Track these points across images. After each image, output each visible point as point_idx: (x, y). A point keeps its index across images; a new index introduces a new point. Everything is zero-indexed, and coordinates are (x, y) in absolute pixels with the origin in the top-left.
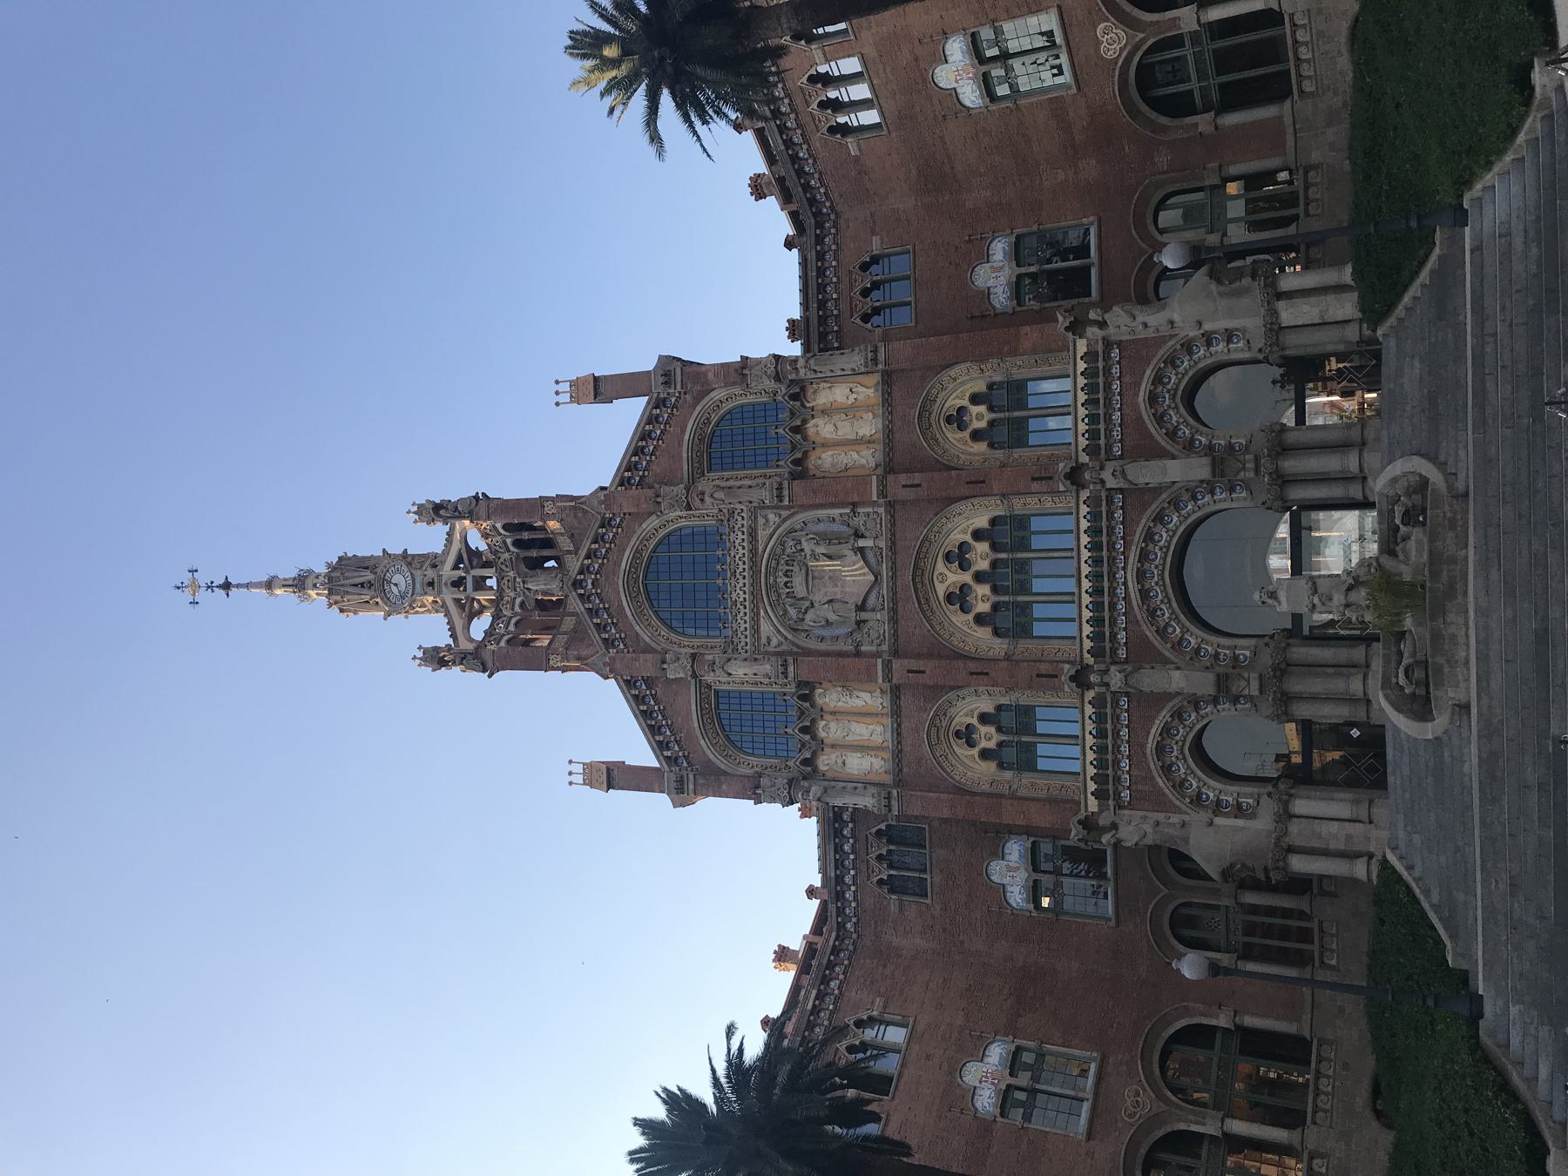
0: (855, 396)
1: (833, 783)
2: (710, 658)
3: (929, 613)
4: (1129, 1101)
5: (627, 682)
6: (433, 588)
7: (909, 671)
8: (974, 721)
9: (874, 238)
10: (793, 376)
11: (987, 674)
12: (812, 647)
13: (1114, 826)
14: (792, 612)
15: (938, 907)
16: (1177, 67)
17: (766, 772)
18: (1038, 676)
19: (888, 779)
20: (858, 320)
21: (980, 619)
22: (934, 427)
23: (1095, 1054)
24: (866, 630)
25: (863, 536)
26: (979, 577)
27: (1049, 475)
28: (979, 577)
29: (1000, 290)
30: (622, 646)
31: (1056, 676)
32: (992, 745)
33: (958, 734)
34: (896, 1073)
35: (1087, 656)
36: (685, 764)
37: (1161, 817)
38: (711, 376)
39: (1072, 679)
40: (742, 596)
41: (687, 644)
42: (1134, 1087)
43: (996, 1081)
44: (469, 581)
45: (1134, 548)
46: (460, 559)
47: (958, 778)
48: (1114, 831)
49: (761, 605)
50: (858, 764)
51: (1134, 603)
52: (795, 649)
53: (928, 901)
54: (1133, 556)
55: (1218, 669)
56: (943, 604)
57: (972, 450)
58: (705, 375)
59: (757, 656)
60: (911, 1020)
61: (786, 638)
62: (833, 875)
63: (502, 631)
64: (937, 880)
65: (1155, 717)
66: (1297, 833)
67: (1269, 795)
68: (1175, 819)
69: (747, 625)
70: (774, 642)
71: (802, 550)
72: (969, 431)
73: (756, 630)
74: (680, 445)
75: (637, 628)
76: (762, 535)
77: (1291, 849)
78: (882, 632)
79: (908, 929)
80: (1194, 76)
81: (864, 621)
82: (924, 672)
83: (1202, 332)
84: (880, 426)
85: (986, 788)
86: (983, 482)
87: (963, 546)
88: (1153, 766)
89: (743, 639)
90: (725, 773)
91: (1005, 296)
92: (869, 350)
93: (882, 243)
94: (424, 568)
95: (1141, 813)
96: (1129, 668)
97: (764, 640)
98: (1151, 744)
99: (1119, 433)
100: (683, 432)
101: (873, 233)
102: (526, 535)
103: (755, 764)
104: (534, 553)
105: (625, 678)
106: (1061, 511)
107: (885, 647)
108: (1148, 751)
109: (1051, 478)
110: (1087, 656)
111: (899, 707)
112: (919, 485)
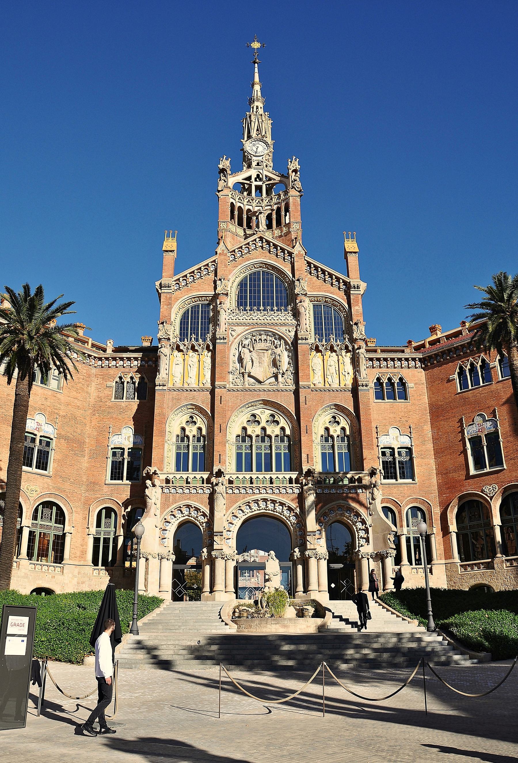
0: (346, 375)
1: (168, 359)
2: (226, 302)
3: (247, 406)
4: (33, 488)
5: (214, 261)
6: (256, 165)
7: (221, 397)
8: (198, 425)
9: (413, 384)
10: (356, 347)
11: (220, 432)
12: (231, 351)
13: (154, 486)
14: (246, 342)
15: (110, 404)
16: (476, 516)
17: (172, 327)
18: (220, 455)
19: (170, 385)
20: (377, 376)
21: (244, 429)
22: (331, 411)
23: (51, 473)
24: (239, 377)
25: (282, 377)
26: (264, 429)
27: (309, 462)
28: (264, 429)
29: (388, 440)
30: (231, 259)
31: (220, 462)
32: (187, 433)
33: (192, 417)
34: (50, 388)
35: (229, 476)
36: (176, 288)
37: (159, 505)
38: (357, 308)
39: (220, 470)
40: (255, 318)
41: (232, 290)
42: (39, 490)
43: (38, 429)
44: (260, 183)
45: (277, 497)
46: (270, 179)
47: (172, 417)
48: (152, 486)
49: (250, 327)
50: (177, 371)
51: (253, 497)
52: (230, 343)
53: (113, 400)
54: (274, 497)
55: (224, 531)
56: (251, 412)
57: (320, 427)
58: (357, 305)
59: (227, 324)
60: (61, 391)
61: (235, 339)
62: (124, 356)
63: (237, 200)
64: (123, 405)
65: (202, 504)
66: (154, 563)
67: (169, 551)
68: (158, 513)
69: (241, 320)
70: (233, 333)
71: (276, 348)
72: (329, 426)
73: (238, 325)
74: (325, 291)
75: (240, 267)
76: (283, 329)
77: (147, 559)
78: (238, 384)
79: (100, 390)
80: (471, 523)
81: (243, 376)
82: (221, 403)
83: (369, 527)
84: (332, 386)
85: (168, 429)
86: (307, 433)
87: (278, 423)
88: (181, 503)
89: (234, 318)
90: (171, 308)
91: (386, 442)
92: (366, 382)
93: (411, 388)
94: (266, 161)
95: (160, 498)
96: (224, 495)
97: (235, 328)
98: (189, 502)
99: (327, 492)
100: (331, 293)
101: (416, 384)
102: (283, 213)
103: (176, 322)
104: (274, 216)
105: (216, 260)
106: (292, 466)
107: (231, 386)
108: (187, 501)
109: (308, 462)
110: (229, 476)
111: (203, 391)
112: (306, 404)
